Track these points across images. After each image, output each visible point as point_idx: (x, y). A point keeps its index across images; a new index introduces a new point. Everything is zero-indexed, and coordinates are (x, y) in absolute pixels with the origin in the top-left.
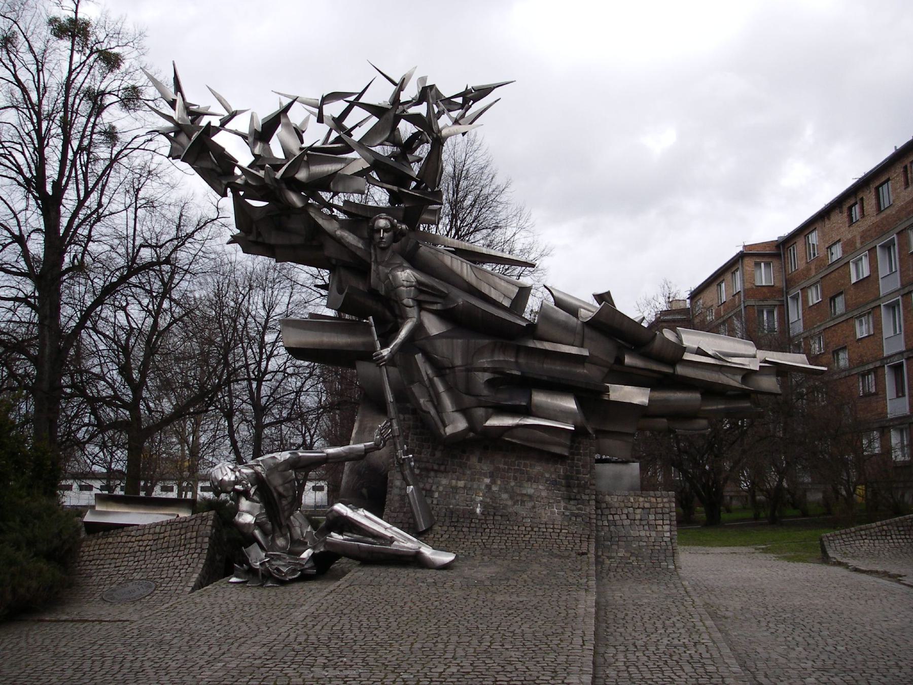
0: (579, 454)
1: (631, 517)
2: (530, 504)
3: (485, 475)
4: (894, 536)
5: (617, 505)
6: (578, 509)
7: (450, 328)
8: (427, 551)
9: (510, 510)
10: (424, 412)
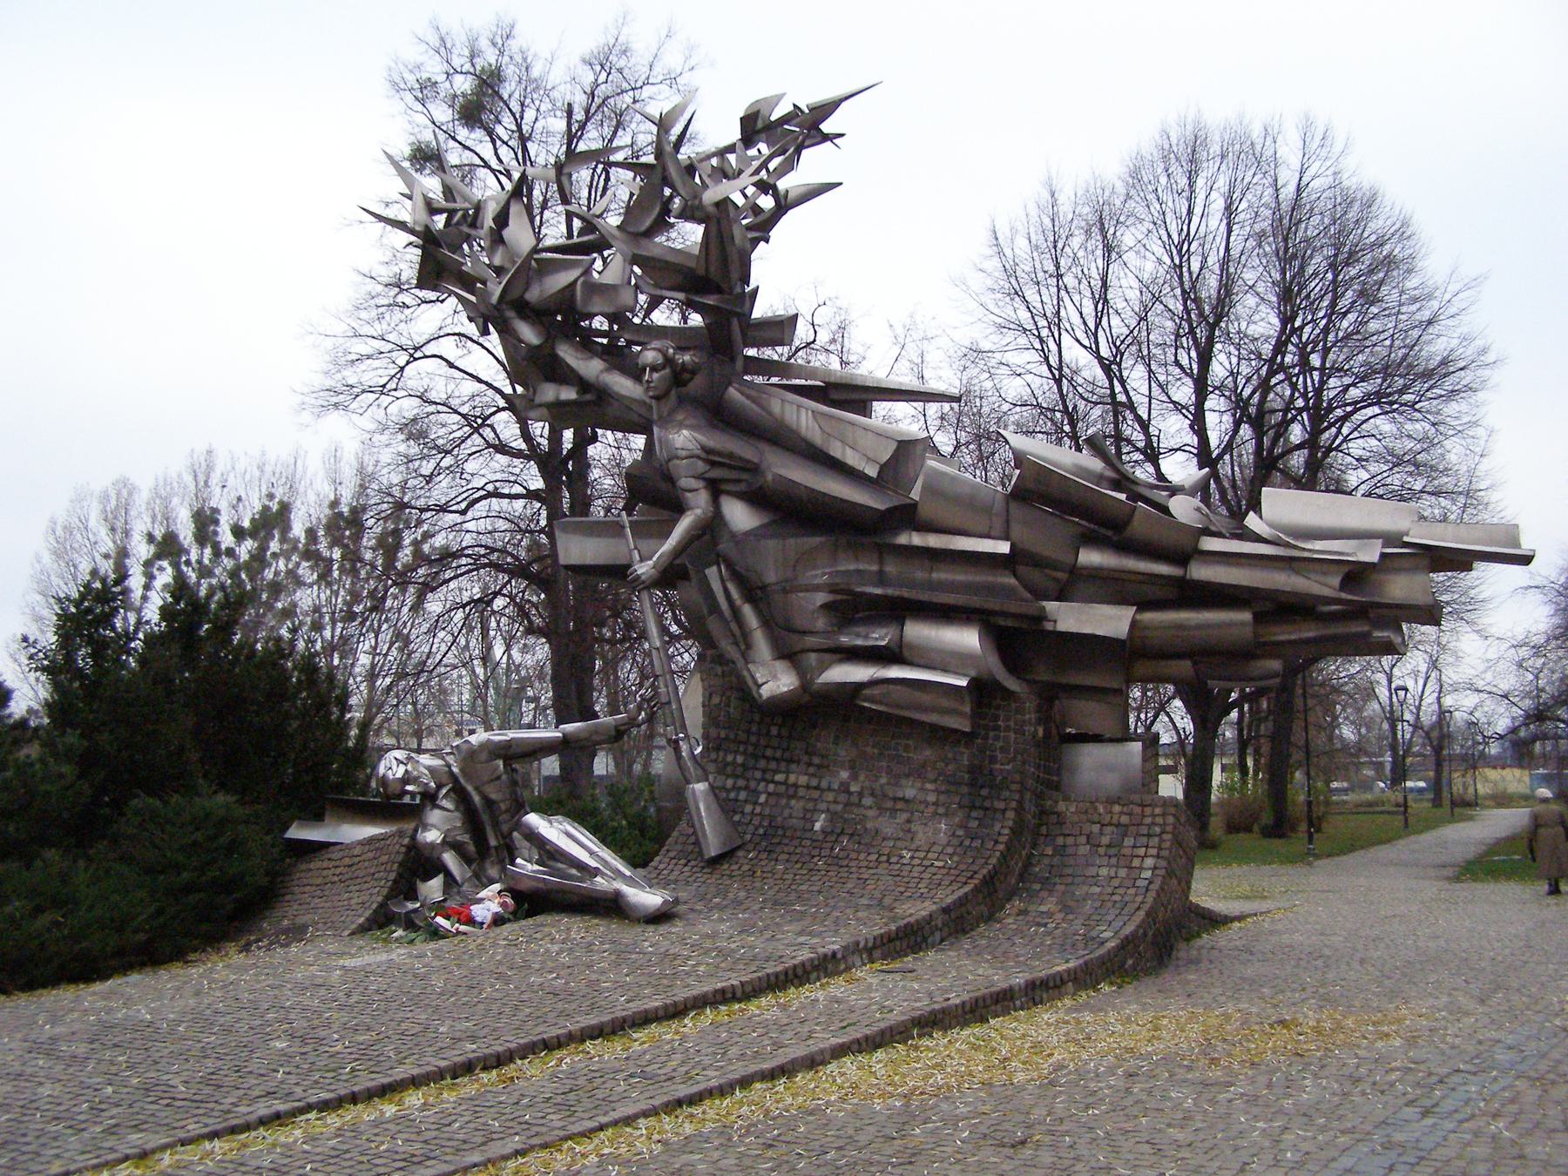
0: (996, 728)
3: (842, 767)
5: (1076, 819)
7: (766, 520)
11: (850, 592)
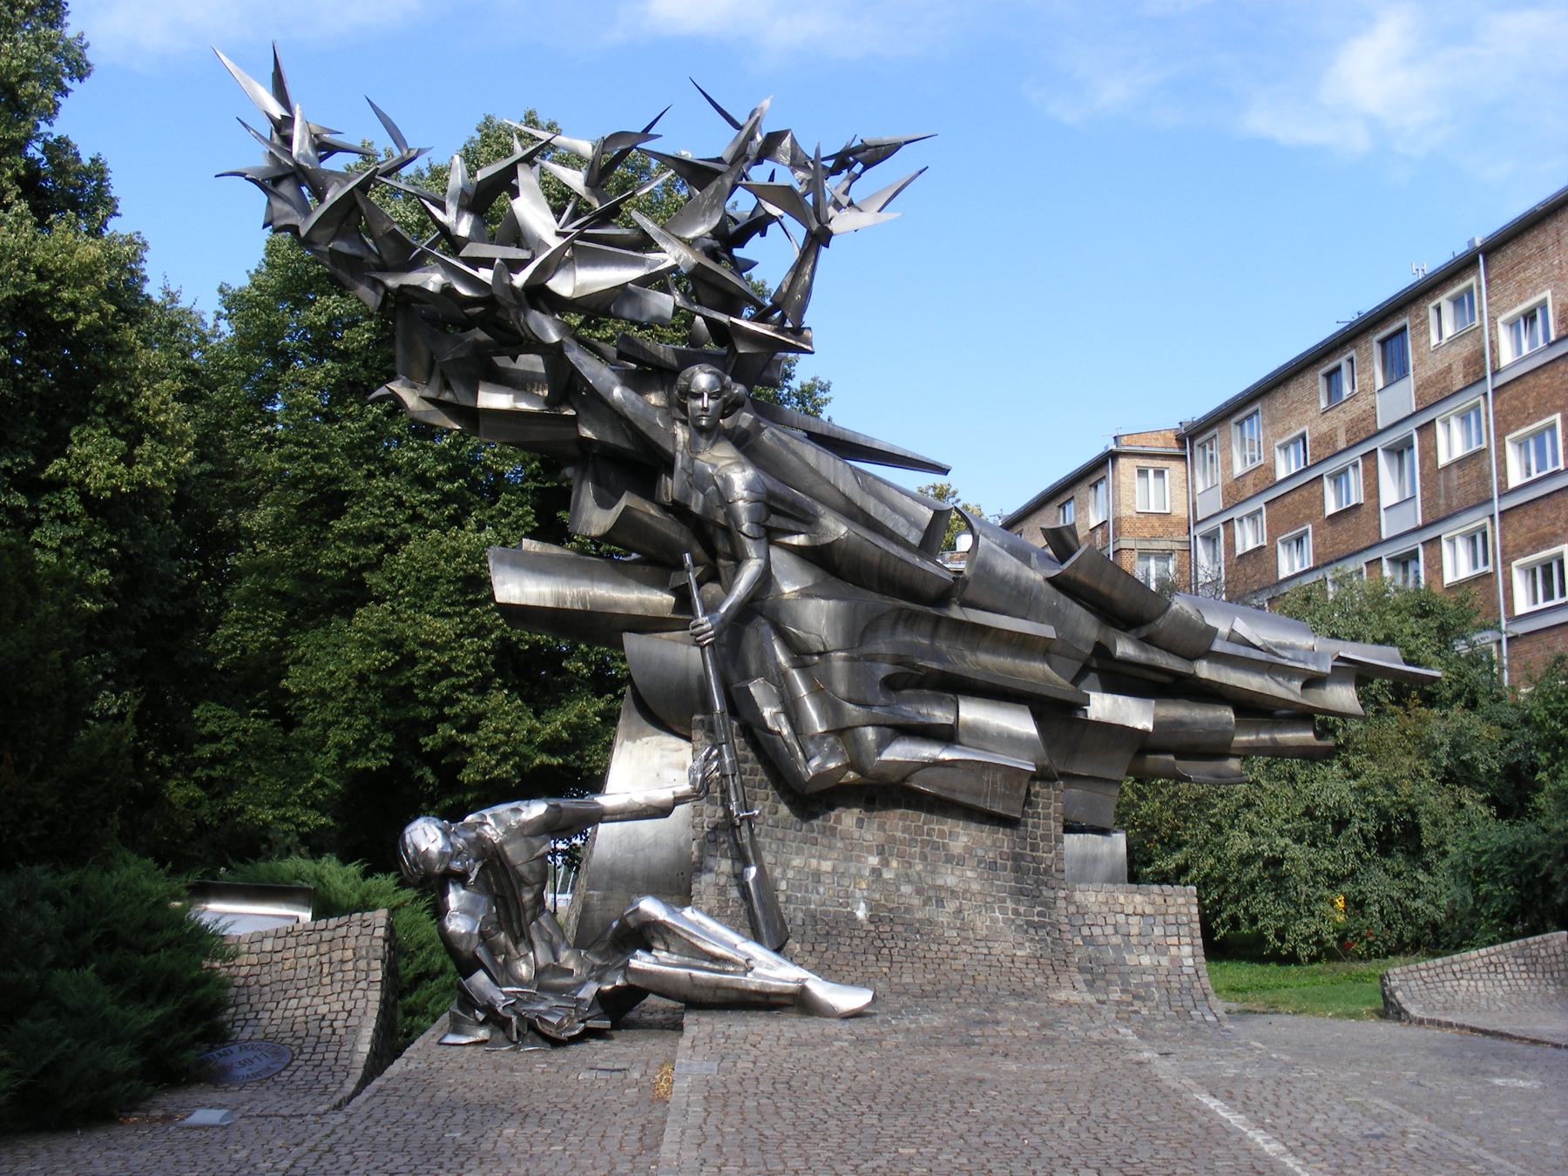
1: (1123, 930)
2: (951, 906)
3: (869, 851)
4: (1509, 975)
5: (1095, 909)
6: (1040, 914)
8: (822, 990)
9: (919, 915)
10: (771, 732)
11: (912, 666)
